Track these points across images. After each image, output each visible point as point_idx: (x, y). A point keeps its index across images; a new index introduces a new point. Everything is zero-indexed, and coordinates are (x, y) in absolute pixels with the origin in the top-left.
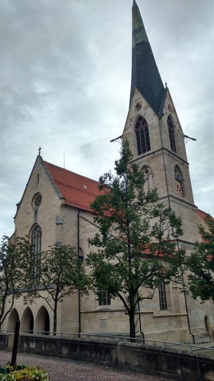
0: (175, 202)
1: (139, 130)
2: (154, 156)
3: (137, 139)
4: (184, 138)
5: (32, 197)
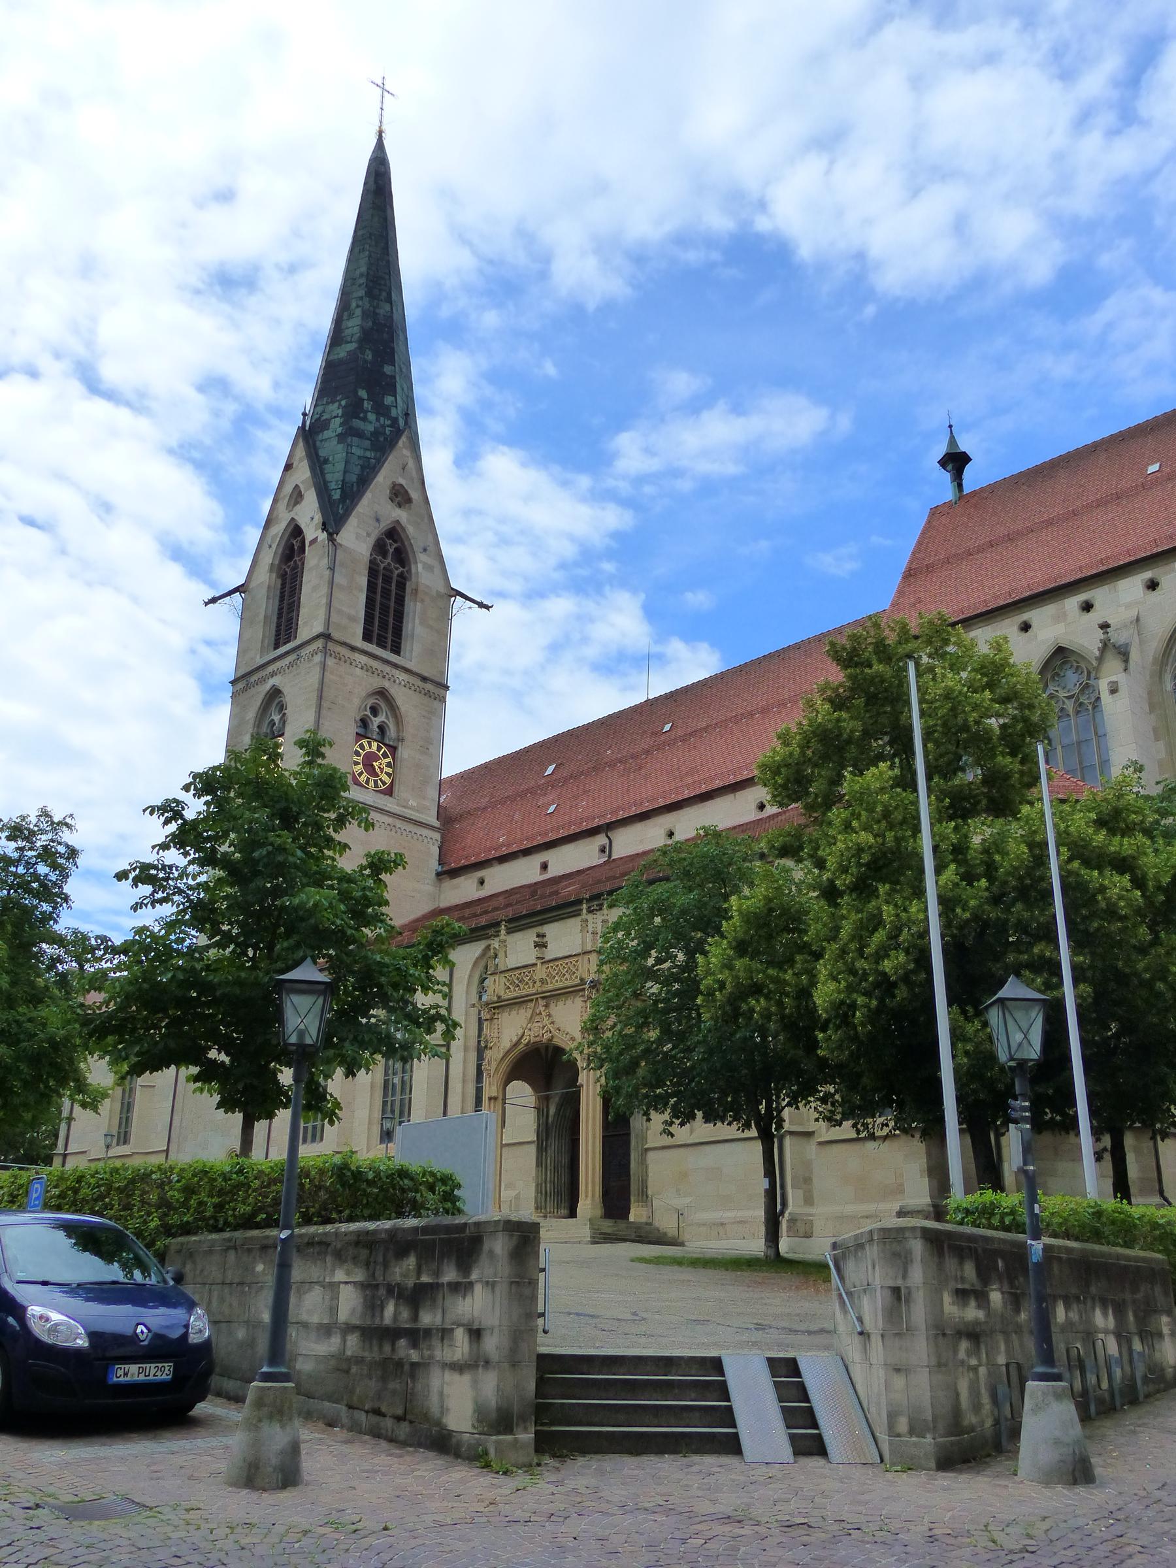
1: (288, 570)
4: (453, 599)
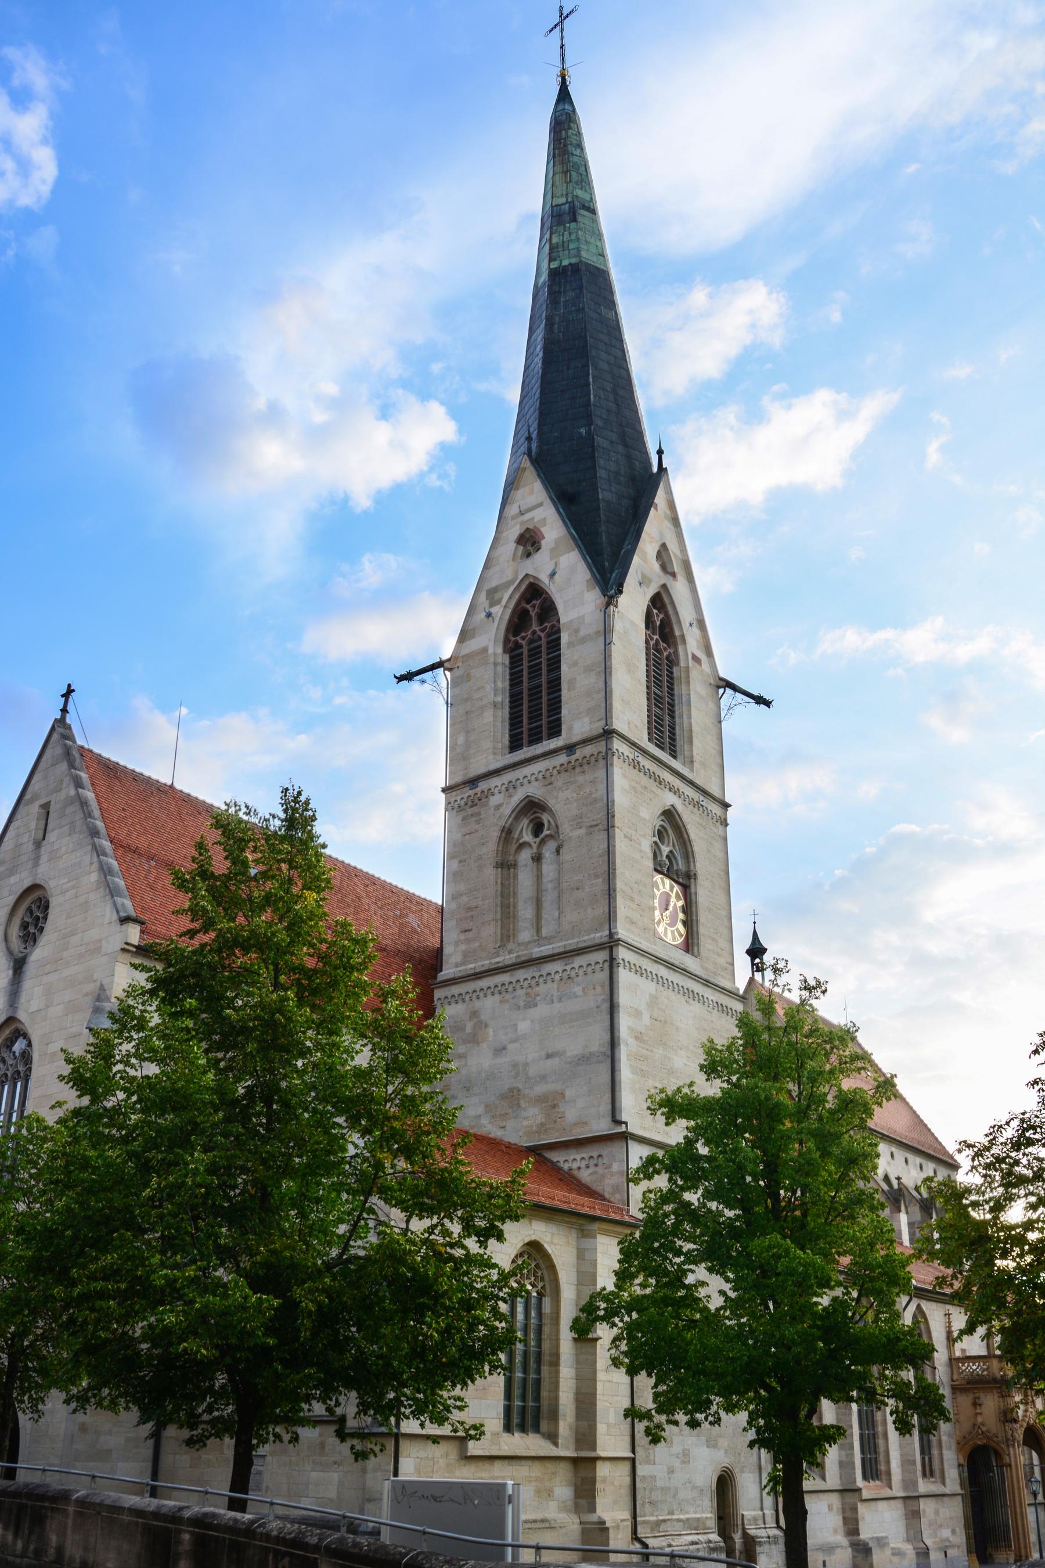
0: (639, 971)
1: (524, 643)
2: (570, 762)
3: (511, 680)
4: (721, 691)
5: (11, 900)
